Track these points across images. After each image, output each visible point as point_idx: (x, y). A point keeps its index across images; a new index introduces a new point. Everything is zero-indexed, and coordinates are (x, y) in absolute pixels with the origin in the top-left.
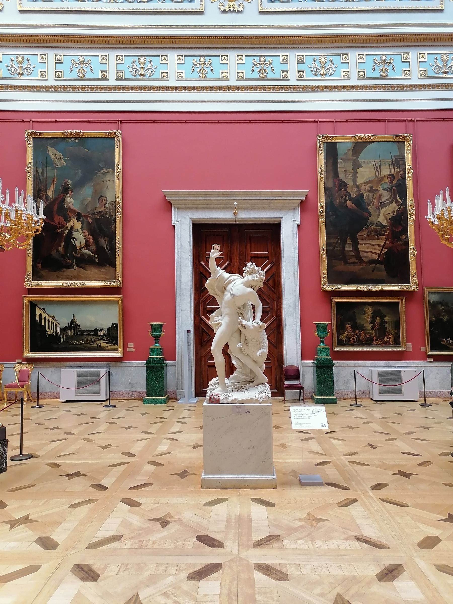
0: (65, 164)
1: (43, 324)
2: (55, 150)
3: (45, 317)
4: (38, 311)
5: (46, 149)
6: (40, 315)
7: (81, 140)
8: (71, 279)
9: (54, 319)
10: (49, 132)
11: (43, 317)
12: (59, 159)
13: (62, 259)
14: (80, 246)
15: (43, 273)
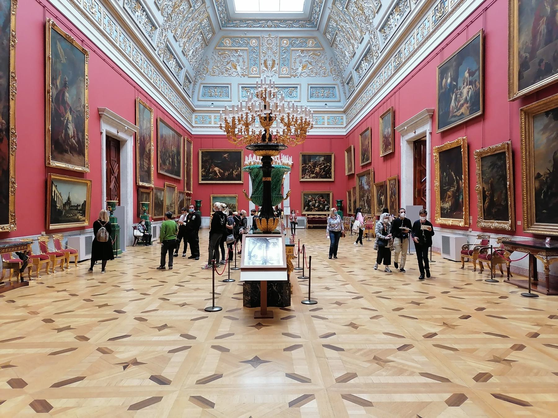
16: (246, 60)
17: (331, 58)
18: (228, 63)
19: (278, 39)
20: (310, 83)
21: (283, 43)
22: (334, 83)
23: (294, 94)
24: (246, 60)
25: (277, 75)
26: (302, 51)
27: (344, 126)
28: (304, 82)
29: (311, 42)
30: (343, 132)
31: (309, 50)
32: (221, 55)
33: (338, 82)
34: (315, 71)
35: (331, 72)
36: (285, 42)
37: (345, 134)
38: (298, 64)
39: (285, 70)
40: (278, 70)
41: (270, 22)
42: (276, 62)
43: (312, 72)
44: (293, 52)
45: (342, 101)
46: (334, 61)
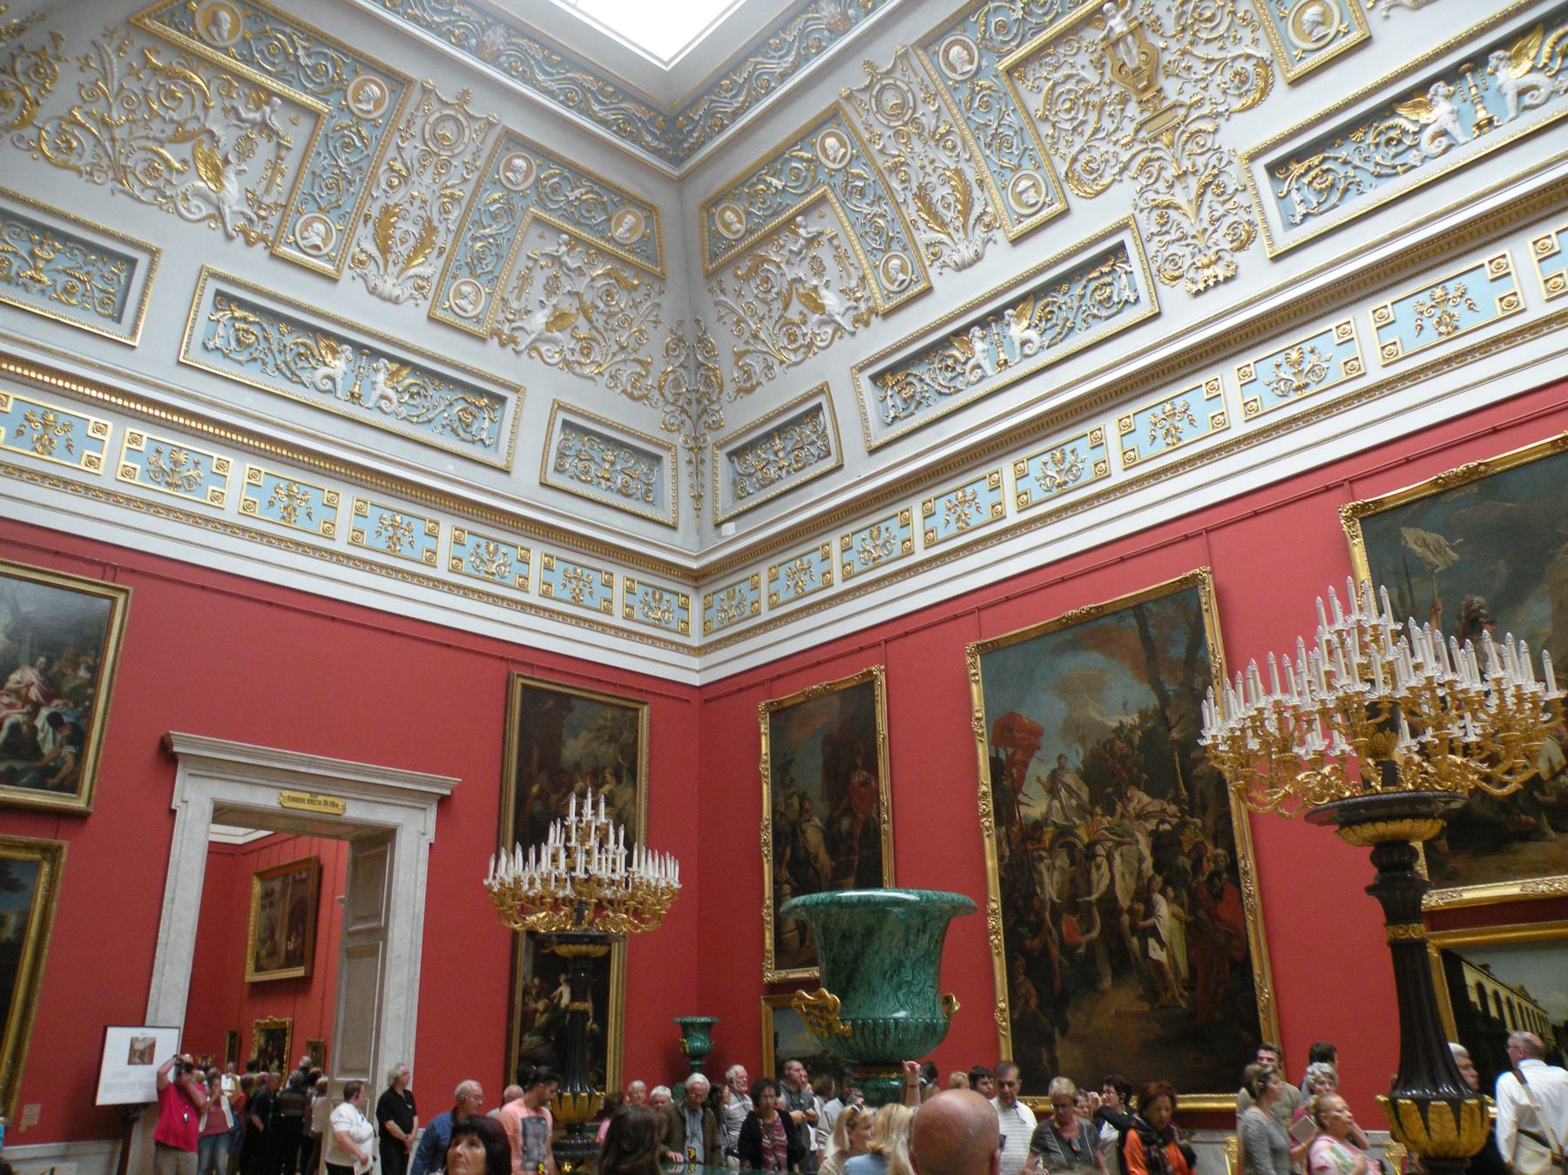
0: (1455, 556)
1: (1494, 1012)
2: (1421, 533)
3: (1496, 994)
4: (1471, 977)
5: (1400, 537)
6: (1480, 987)
7: (1483, 481)
8: (1546, 872)
9: (1526, 997)
10: (1396, 492)
11: (1489, 991)
12: (1439, 551)
13: (1503, 817)
14: (1552, 768)
15: (1458, 863)
16: (290, 163)
17: (680, 323)
18: (180, 136)
19: (498, 130)
20: (566, 399)
21: (509, 167)
22: (663, 436)
23: (482, 427)
24: (290, 163)
25: (425, 306)
26: (575, 241)
27: (695, 640)
28: (540, 387)
29: (629, 220)
30: (692, 672)
31: (601, 252)
32: (155, 69)
33: (679, 440)
34: (596, 355)
35: (661, 388)
36: (519, 162)
37: (697, 680)
38: (536, 291)
39: (469, 298)
40: (434, 281)
41: (500, 30)
42: (441, 239)
43: (586, 351)
44: (536, 231)
45: (681, 527)
46: (692, 345)
